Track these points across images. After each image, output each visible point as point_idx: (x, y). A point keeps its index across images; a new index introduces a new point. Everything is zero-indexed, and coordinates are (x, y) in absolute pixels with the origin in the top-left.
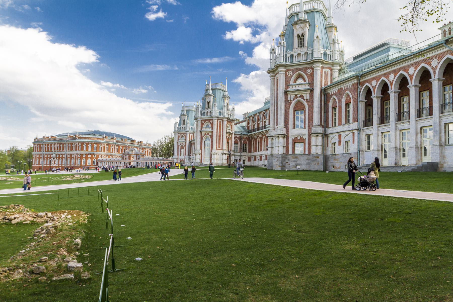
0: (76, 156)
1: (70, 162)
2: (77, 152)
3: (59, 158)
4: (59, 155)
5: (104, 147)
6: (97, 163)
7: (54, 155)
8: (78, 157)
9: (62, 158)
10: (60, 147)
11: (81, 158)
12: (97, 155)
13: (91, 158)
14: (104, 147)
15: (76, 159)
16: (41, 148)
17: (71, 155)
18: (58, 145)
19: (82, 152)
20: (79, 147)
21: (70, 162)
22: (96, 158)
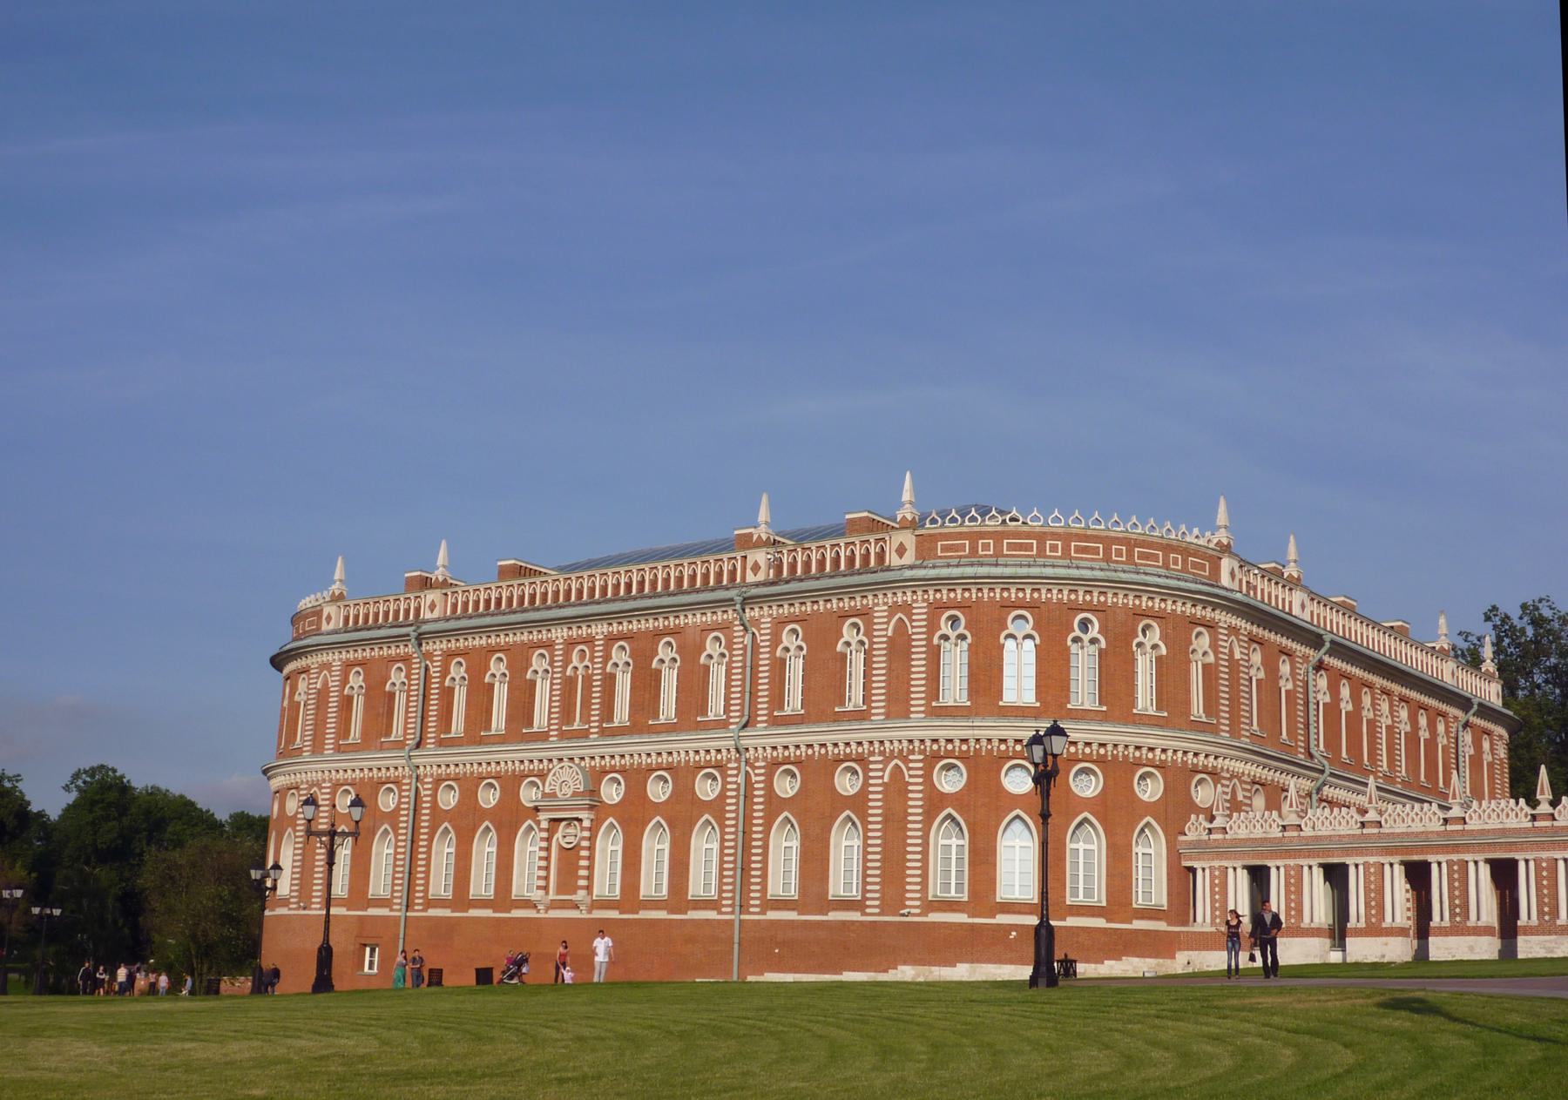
0: (897, 788)
1: (814, 861)
2: (919, 728)
3: (634, 815)
4: (636, 777)
6: (1182, 878)
7: (566, 781)
8: (935, 802)
9: (683, 815)
10: (646, 685)
11: (982, 812)
13: (1117, 814)
15: (895, 821)
16: (381, 704)
17: (817, 770)
18: (620, 656)
20: (934, 656)
21: (814, 861)
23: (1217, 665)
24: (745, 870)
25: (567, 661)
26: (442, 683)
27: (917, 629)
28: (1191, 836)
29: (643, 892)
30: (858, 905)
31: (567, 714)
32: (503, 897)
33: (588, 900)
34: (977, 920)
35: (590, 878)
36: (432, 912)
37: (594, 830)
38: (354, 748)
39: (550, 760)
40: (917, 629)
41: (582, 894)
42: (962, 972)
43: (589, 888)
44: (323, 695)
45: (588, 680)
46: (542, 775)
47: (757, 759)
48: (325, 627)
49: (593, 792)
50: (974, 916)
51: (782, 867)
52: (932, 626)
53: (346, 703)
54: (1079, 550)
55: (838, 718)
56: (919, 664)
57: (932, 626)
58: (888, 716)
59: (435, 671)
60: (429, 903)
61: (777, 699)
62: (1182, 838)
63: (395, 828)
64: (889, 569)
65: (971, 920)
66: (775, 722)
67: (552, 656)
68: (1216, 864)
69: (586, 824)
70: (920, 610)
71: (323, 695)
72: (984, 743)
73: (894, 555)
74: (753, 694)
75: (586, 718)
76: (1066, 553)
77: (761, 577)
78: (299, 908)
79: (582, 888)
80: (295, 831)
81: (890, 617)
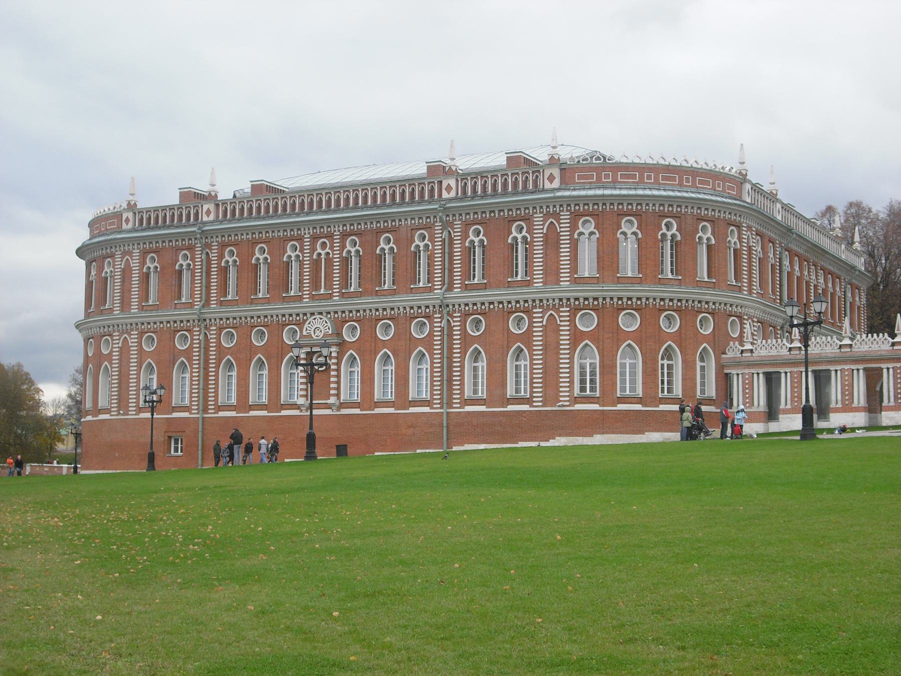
0: (552, 328)
3: (368, 349)
4: (368, 322)
5: (750, 248)
6: (725, 381)
8: (577, 337)
9: (403, 348)
10: (372, 265)
12: (720, 316)
14: (750, 248)
15: (551, 349)
16: (173, 278)
19: (610, 290)
20: (574, 245)
22: (719, 341)
23: (741, 250)
24: (450, 381)
25: (313, 249)
26: (219, 264)
27: (563, 228)
28: (730, 354)
29: (376, 397)
30: (528, 401)
31: (315, 285)
32: (275, 403)
33: (337, 403)
34: (605, 408)
35: (338, 389)
36: (221, 414)
37: (339, 358)
38: (155, 307)
39: (305, 314)
40: (563, 228)
41: (332, 400)
42: (598, 439)
43: (338, 395)
44: (126, 273)
45: (329, 261)
46: (300, 324)
47: (455, 312)
48: (124, 226)
49: (339, 334)
50: (603, 406)
51: (474, 378)
52: (573, 227)
53: (145, 278)
54: (664, 178)
55: (510, 285)
56: (565, 250)
57: (573, 227)
58: (545, 283)
59: (214, 256)
60: (219, 408)
61: (468, 273)
62: (723, 356)
63: (190, 360)
64: (544, 191)
65: (601, 408)
66: (466, 288)
67: (302, 246)
68: (747, 371)
69: (334, 354)
70: (565, 216)
71: (126, 273)
72: (608, 300)
73: (546, 182)
74: (451, 271)
75: (329, 286)
76: (656, 181)
77: (453, 194)
78: (119, 414)
79: (334, 395)
80: (111, 364)
81: (545, 221)
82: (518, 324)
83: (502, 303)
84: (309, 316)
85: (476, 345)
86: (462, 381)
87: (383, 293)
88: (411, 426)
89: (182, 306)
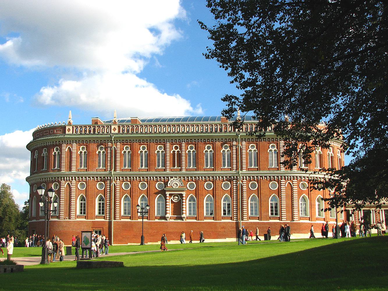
69: (184, 195)
82: (303, 185)
83: (266, 177)
84: (170, 178)
85: (209, 194)
86: (76, 208)
87: (207, 170)
88: (223, 228)
89: (100, 170)
